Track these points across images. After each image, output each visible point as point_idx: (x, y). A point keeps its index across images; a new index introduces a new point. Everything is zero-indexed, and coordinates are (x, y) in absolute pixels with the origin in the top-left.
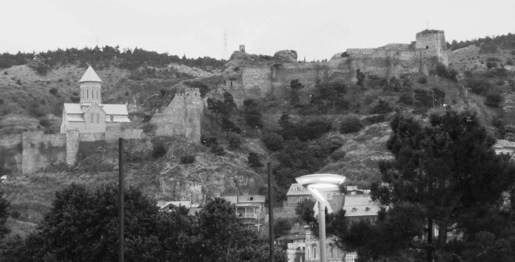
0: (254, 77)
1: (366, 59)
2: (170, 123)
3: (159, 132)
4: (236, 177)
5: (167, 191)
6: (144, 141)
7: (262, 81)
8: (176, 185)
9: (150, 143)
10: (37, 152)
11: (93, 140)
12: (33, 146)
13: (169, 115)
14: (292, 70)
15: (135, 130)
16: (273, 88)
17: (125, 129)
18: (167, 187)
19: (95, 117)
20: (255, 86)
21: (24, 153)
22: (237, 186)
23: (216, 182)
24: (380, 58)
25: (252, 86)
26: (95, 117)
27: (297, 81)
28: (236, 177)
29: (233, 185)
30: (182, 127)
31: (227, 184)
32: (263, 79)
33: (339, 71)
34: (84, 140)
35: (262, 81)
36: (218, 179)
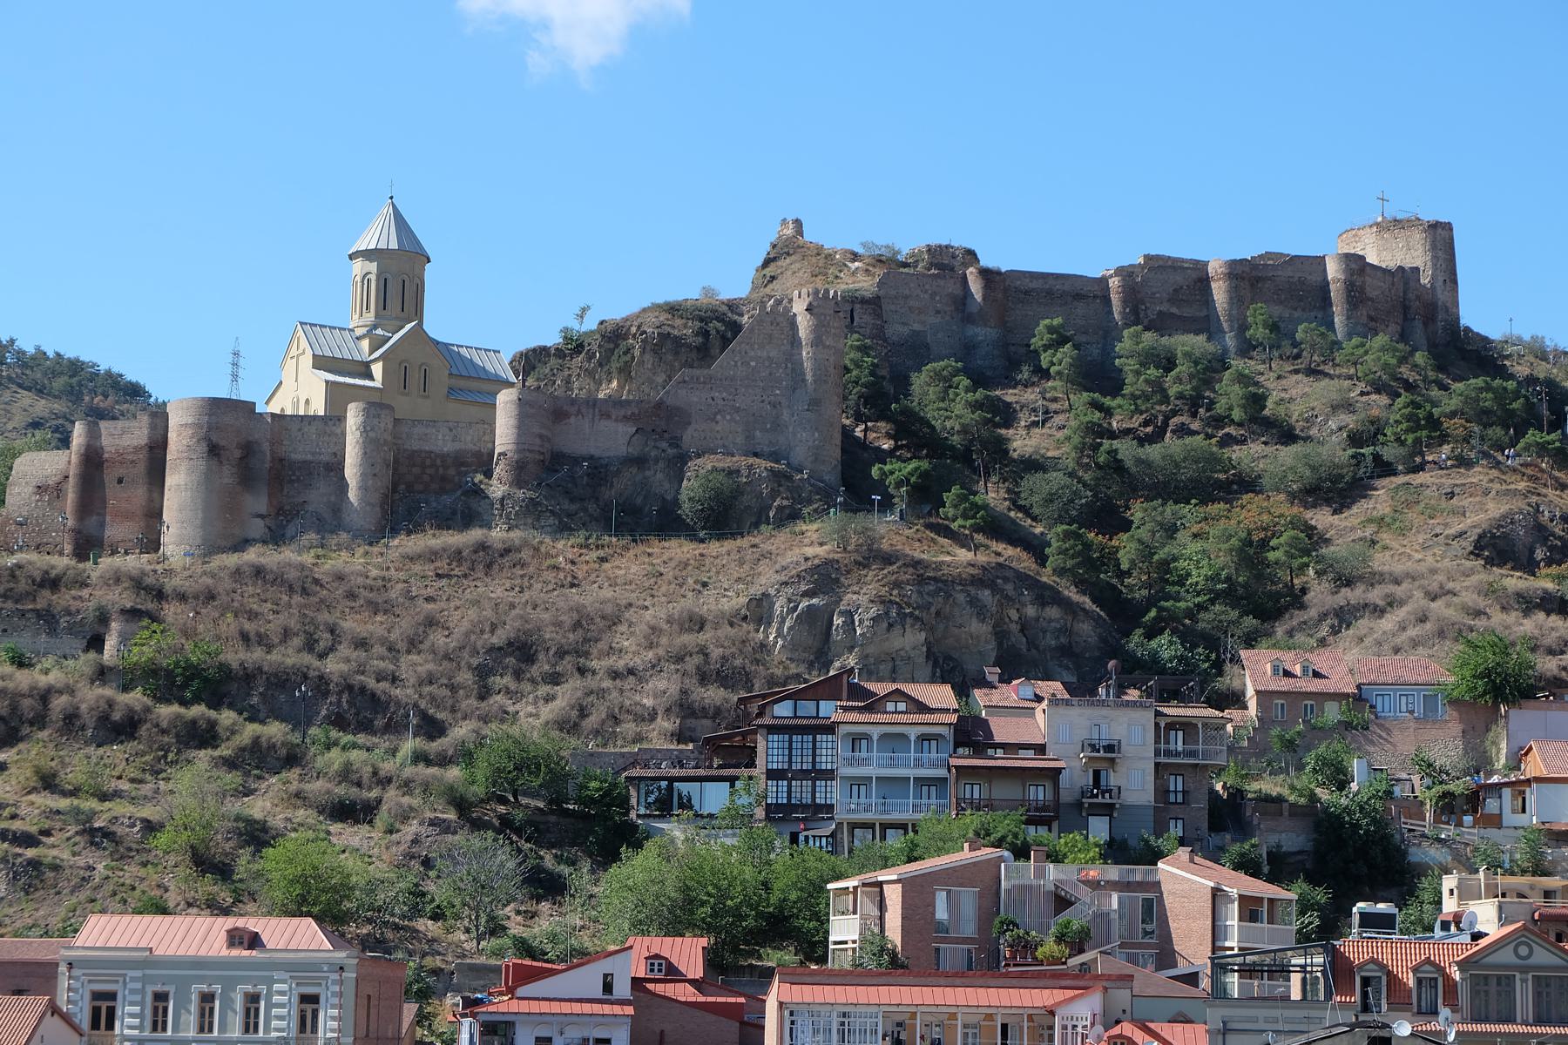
0: (912, 303)
1: (1258, 279)
2: (737, 410)
4: (1031, 611)
6: (640, 461)
7: (937, 320)
9: (659, 476)
10: (228, 476)
13: (732, 379)
14: (1026, 293)
15: (605, 425)
17: (566, 415)
19: (415, 378)
20: (915, 333)
24: (1302, 282)
25: (905, 330)
26: (415, 378)
30: (777, 426)
31: (1000, 635)
32: (938, 312)
33: (1174, 310)
35: (934, 320)
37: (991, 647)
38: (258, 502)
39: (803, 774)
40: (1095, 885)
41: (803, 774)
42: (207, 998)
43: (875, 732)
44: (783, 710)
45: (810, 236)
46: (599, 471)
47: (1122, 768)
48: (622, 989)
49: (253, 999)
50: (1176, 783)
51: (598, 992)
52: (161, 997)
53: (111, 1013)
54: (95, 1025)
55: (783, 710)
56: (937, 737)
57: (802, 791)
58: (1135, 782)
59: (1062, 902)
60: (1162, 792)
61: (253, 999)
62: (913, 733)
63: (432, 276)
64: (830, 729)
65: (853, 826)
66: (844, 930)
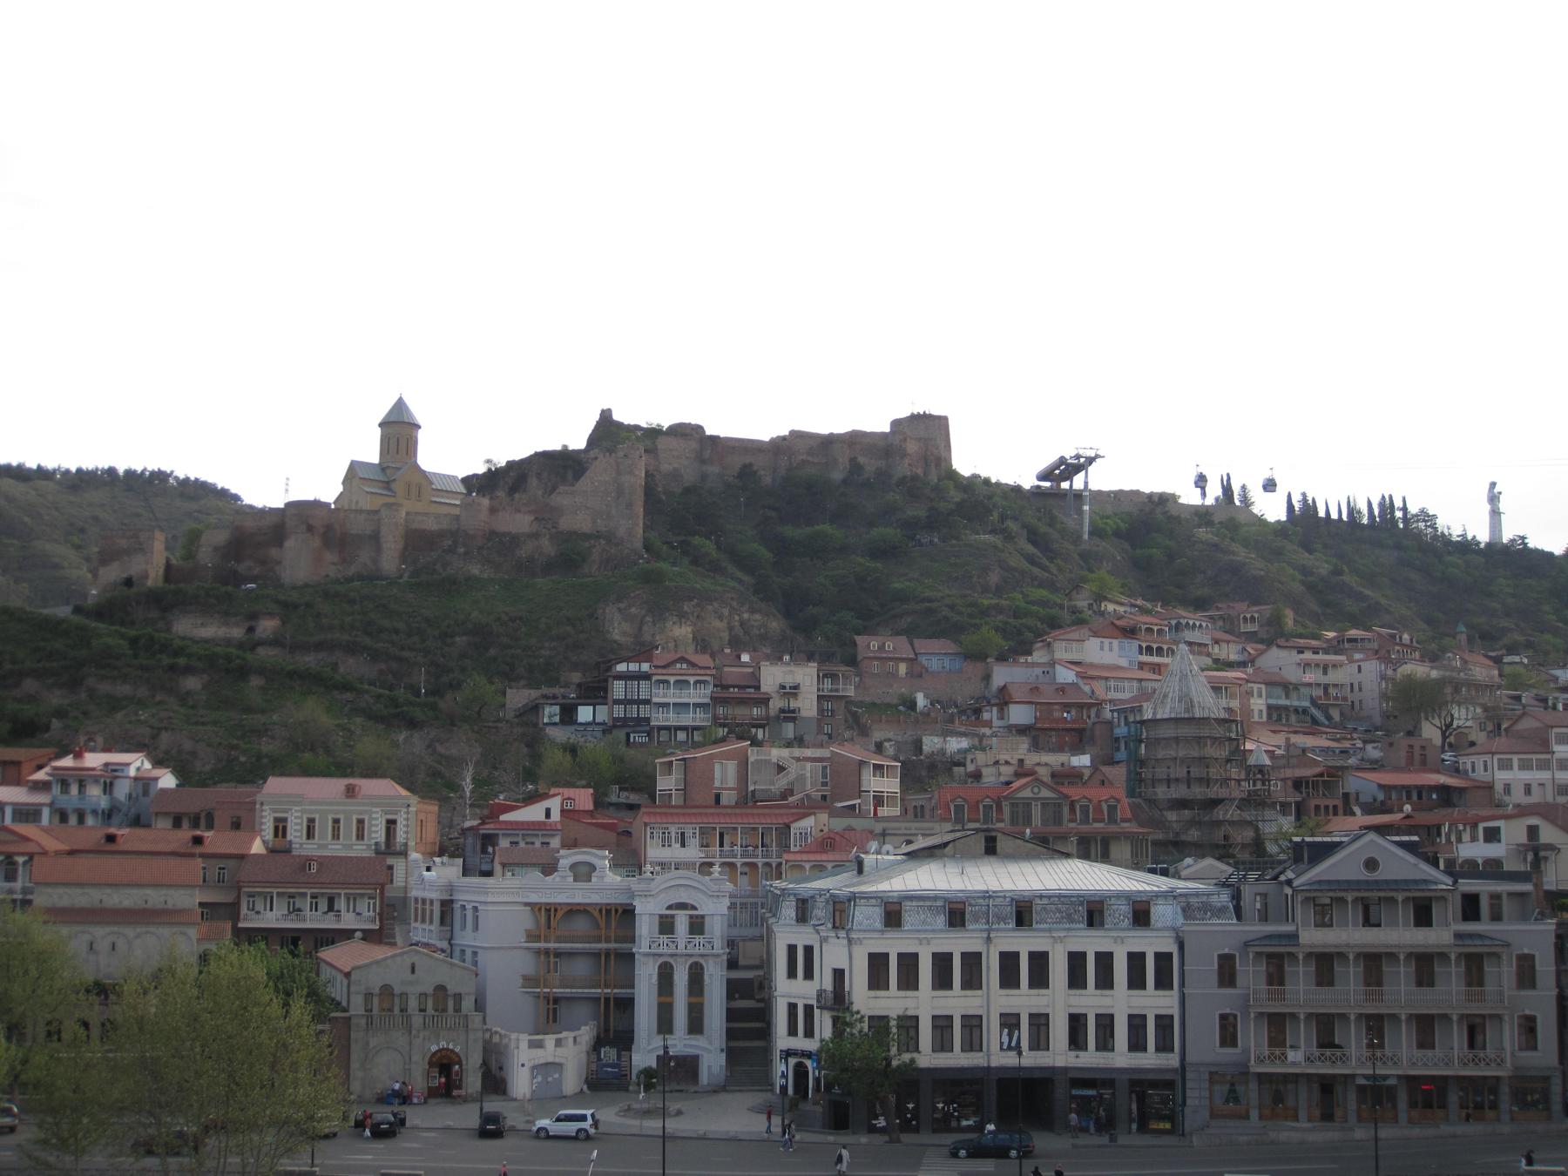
3: (566, 523)
4: (746, 616)
5: (624, 634)
6: (535, 536)
8: (642, 623)
10: (317, 542)
11: (435, 527)
12: (310, 529)
15: (518, 516)
16: (704, 477)
18: (626, 627)
21: (289, 543)
22: (746, 633)
23: (717, 624)
27: (751, 465)
28: (746, 616)
29: (738, 631)
31: (731, 629)
34: (415, 526)
36: (721, 618)
37: (726, 635)
38: (330, 557)
39: (632, 702)
40: (798, 759)
41: (632, 702)
42: (336, 821)
43: (672, 679)
44: (622, 667)
45: (616, 417)
46: (514, 540)
47: (800, 698)
48: (556, 816)
49: (361, 822)
50: (828, 705)
51: (542, 818)
52: (311, 821)
53: (285, 828)
54: (276, 835)
55: (622, 667)
56: (704, 682)
57: (633, 712)
58: (807, 705)
59: (781, 769)
60: (821, 711)
61: (361, 822)
62: (692, 680)
63: (421, 435)
64: (646, 677)
65: (660, 728)
66: (666, 783)
